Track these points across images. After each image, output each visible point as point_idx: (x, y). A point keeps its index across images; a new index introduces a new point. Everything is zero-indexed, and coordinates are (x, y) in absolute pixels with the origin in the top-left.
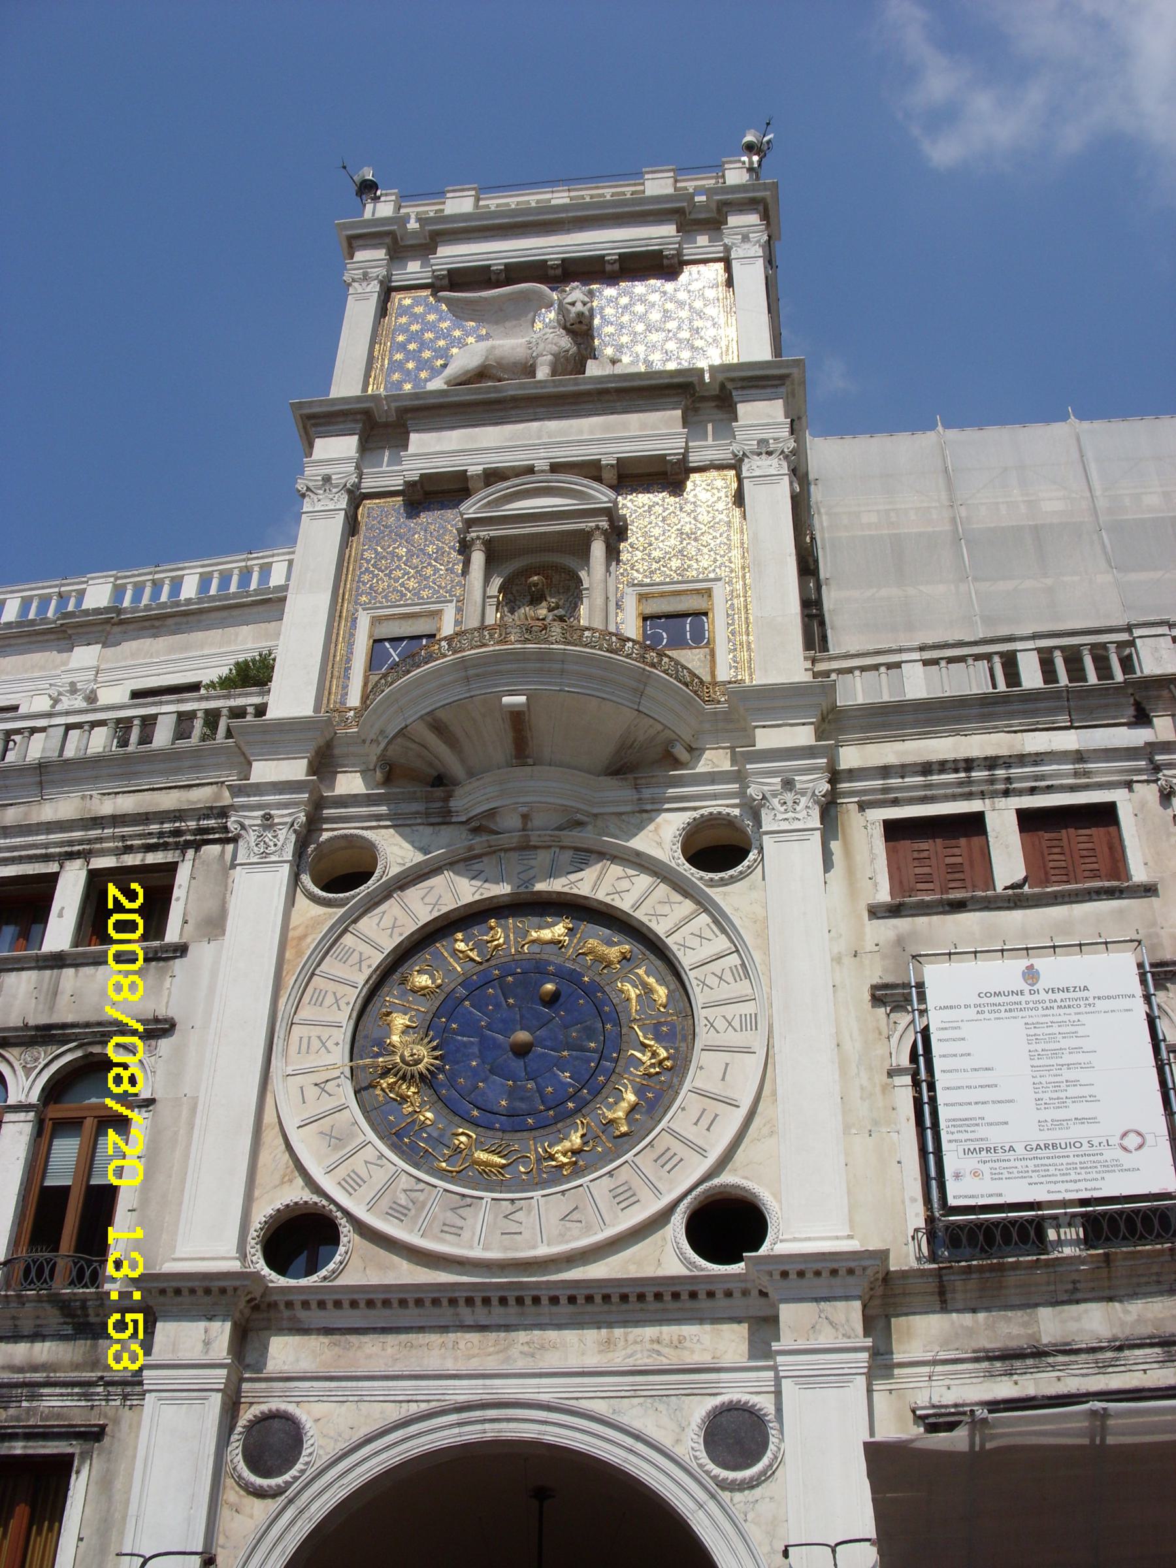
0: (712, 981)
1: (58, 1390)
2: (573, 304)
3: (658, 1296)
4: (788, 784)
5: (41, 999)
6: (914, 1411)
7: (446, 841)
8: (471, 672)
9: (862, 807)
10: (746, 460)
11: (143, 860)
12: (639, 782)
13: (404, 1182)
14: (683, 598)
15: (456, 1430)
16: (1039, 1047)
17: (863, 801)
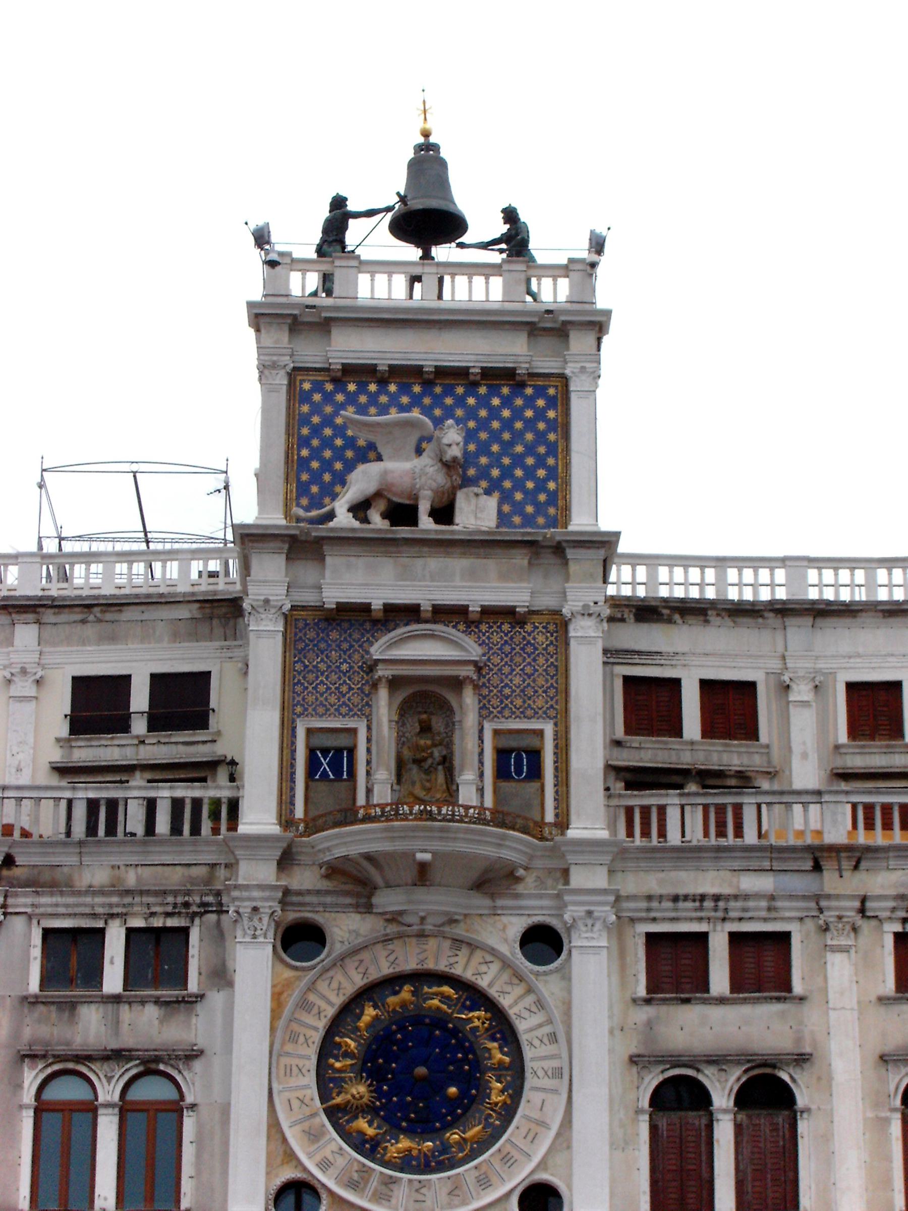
0: (536, 1042)
2: (450, 445)
10: (573, 620)
11: (164, 923)
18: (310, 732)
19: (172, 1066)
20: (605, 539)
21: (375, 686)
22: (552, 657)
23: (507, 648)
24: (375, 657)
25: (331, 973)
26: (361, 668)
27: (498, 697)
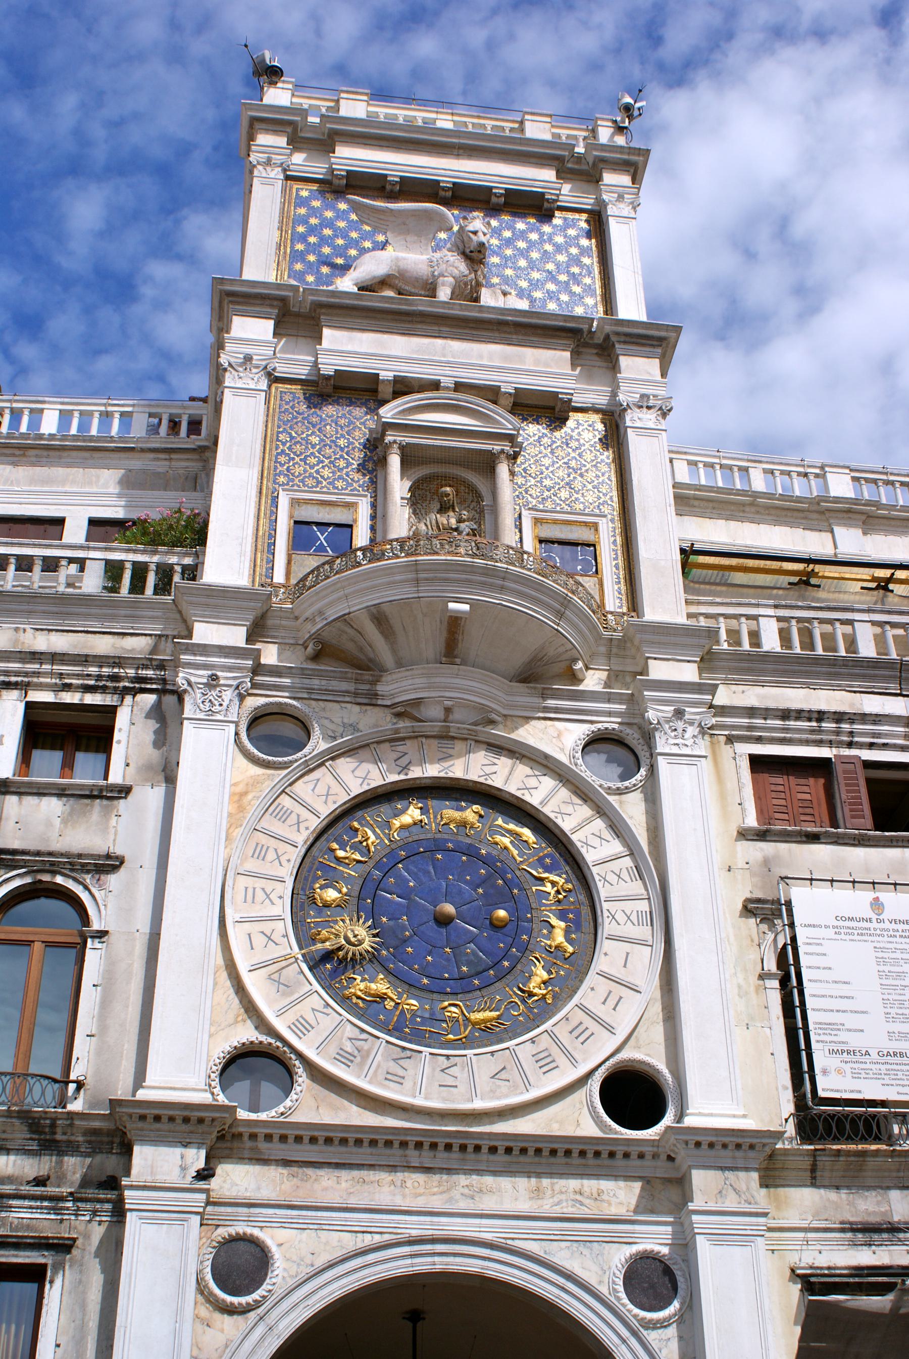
0: (612, 878)
1: (27, 1203)
2: (475, 233)
3: (583, 1153)
4: (679, 714)
6: (793, 1270)
7: (373, 721)
8: (422, 575)
9: (730, 740)
10: (629, 411)
11: (81, 700)
12: (545, 692)
14: (573, 527)
15: (409, 1261)
16: (887, 968)
17: (733, 736)
19: (75, 880)
20: (663, 334)
21: (383, 462)
24: (384, 420)
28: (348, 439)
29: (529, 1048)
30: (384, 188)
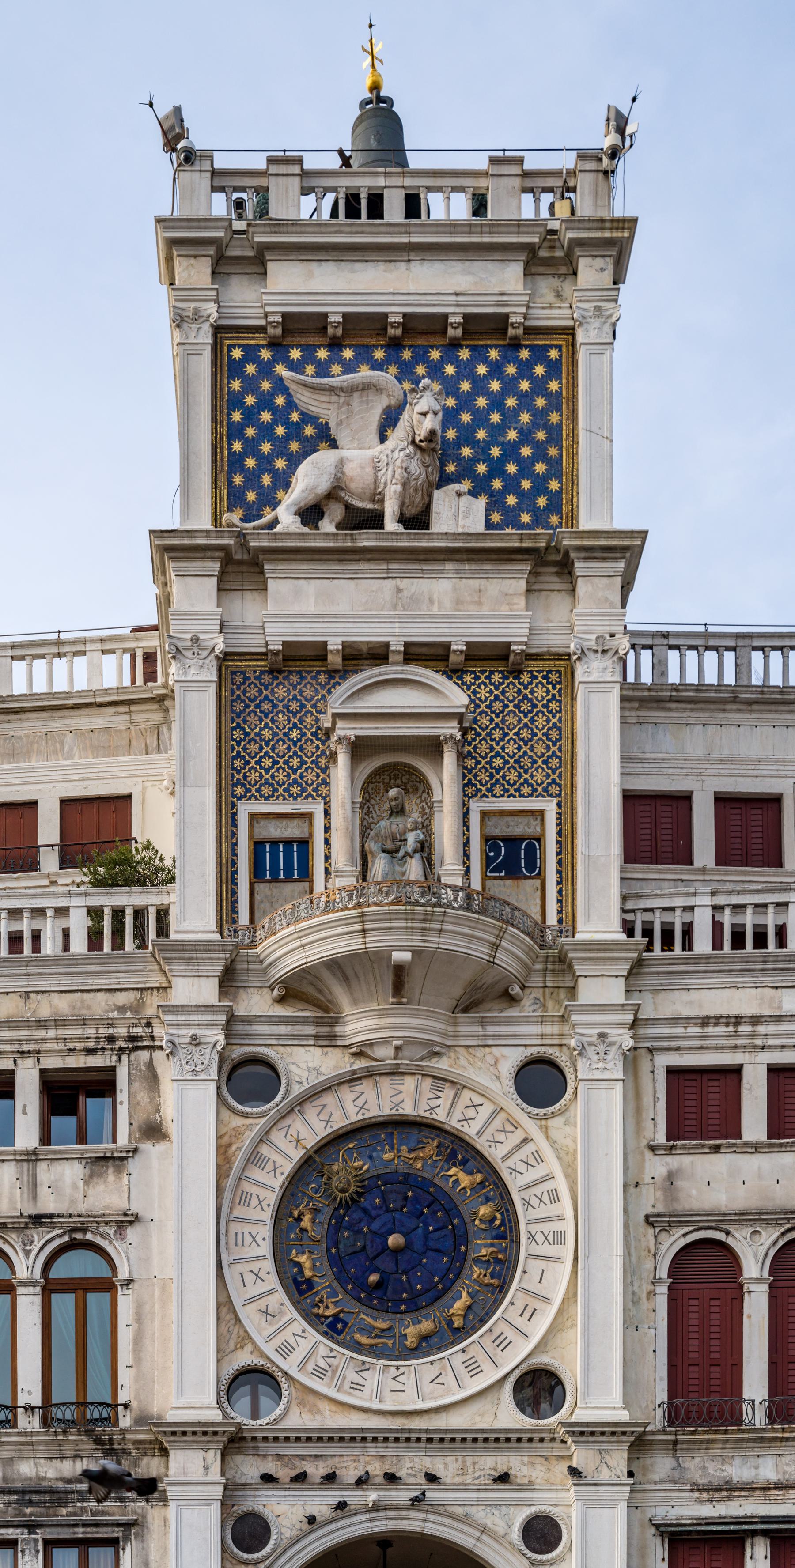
5: (25, 1189)
6: (651, 1520)
13: (322, 1350)
15: (369, 1524)
18: (253, 818)
19: (102, 1236)
22: (554, 717)
23: (498, 706)
25: (288, 1121)
26: (315, 734)
27: (487, 770)
28: (300, 729)
29: (462, 1357)
30: (325, 328)
